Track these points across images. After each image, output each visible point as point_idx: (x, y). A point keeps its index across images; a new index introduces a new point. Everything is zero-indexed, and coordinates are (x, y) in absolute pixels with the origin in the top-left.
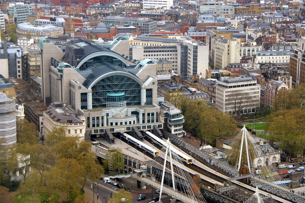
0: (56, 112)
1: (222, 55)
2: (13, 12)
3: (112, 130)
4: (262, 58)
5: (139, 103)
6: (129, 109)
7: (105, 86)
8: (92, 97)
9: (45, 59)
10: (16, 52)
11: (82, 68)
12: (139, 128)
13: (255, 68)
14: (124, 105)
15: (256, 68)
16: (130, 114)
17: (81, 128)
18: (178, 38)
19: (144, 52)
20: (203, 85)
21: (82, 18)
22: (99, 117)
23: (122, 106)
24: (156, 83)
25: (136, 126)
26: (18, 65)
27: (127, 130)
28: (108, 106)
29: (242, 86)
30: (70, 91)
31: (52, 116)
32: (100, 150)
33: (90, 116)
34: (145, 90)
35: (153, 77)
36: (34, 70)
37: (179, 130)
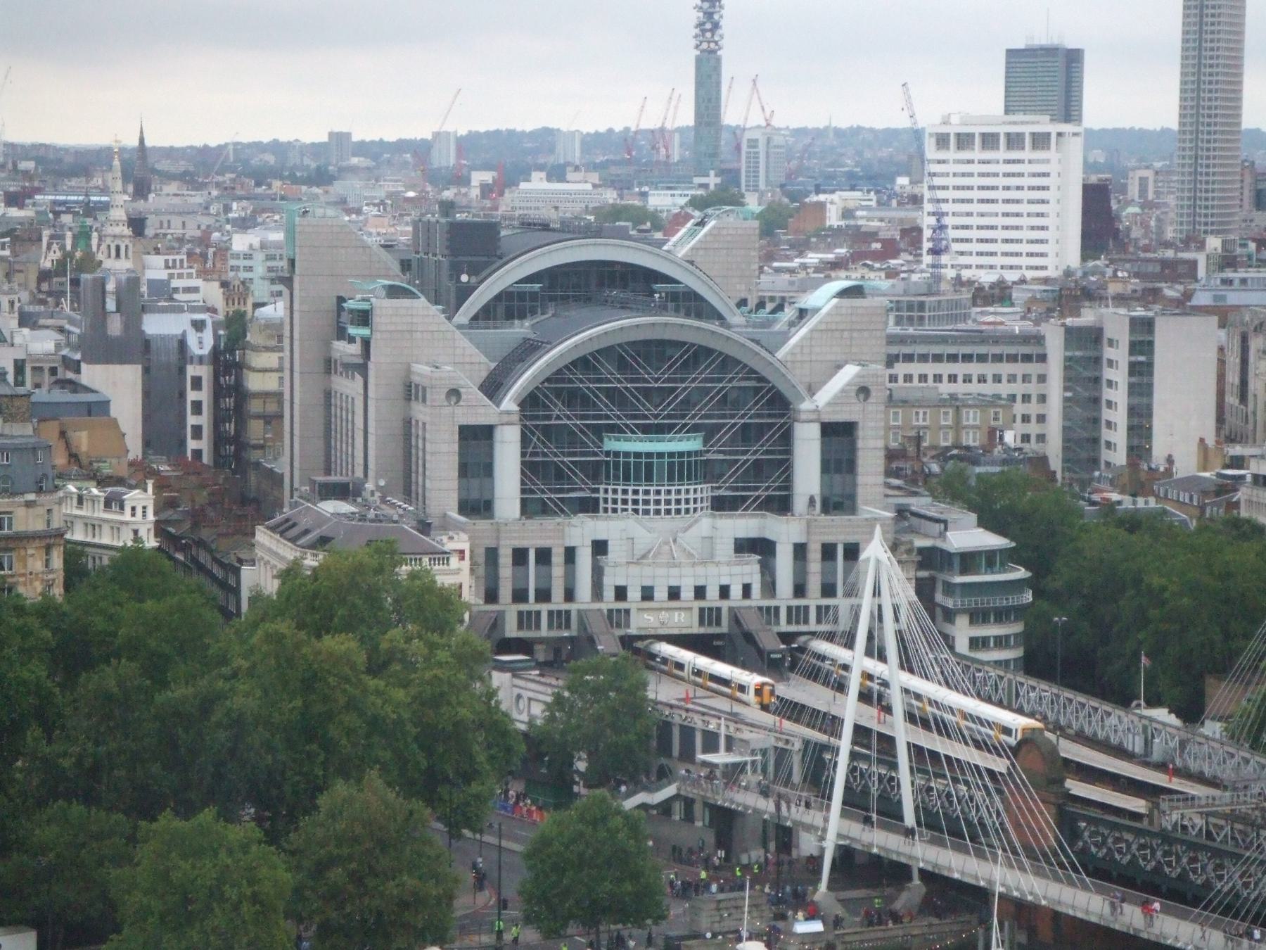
5: (781, 504)
7: (597, 397)
8: (523, 454)
10: (185, 332)
11: (486, 315)
14: (699, 505)
16: (725, 549)
20: (1172, 500)
24: (877, 396)
26: (192, 396)
27: (701, 623)
31: (293, 532)
32: (531, 694)
33: (502, 543)
34: (814, 431)
37: (1001, 642)
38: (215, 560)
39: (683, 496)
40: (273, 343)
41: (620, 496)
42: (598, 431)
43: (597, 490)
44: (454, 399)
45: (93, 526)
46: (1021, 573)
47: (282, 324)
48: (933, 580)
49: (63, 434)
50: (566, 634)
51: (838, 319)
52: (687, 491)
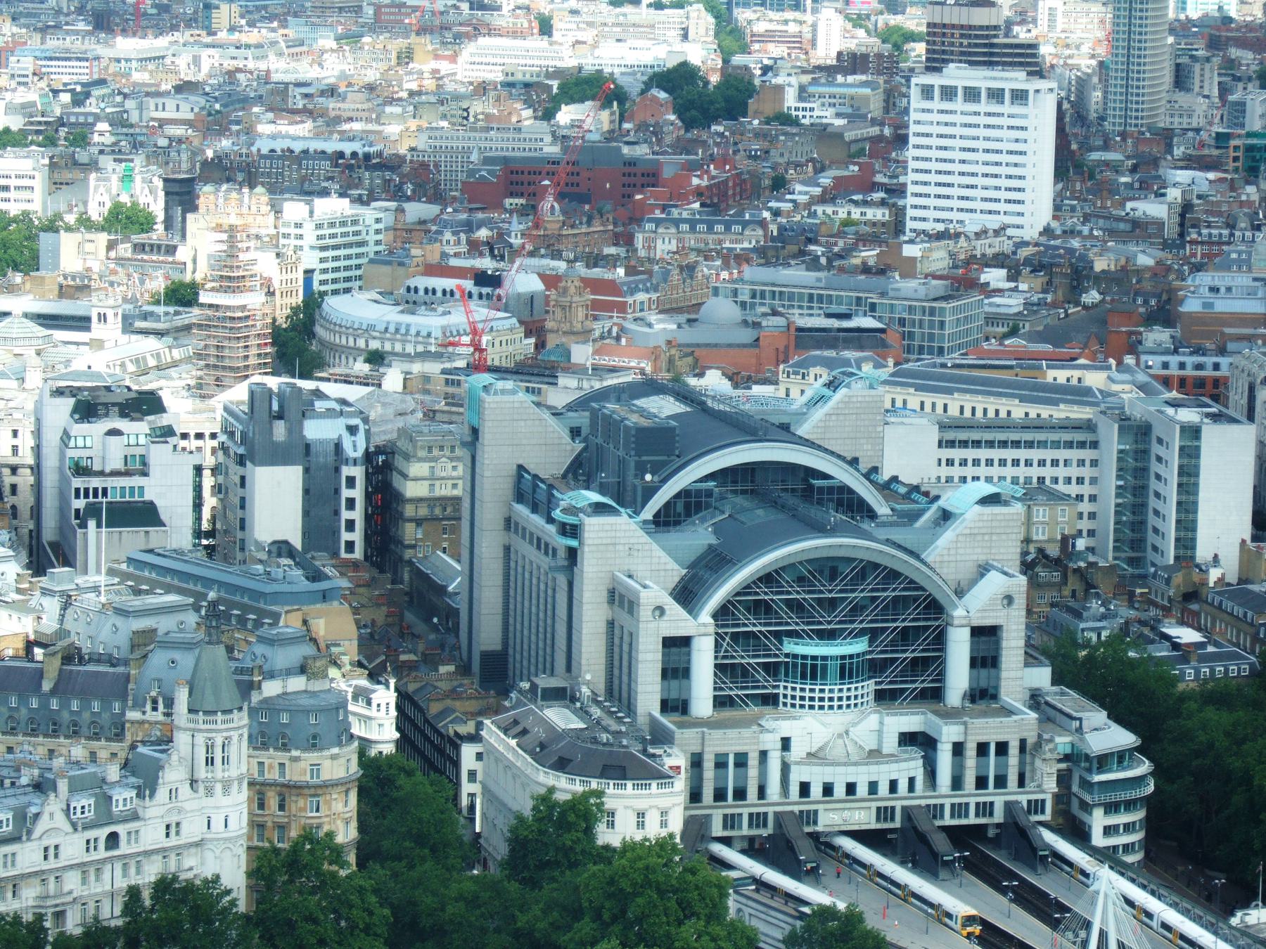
2: (299, 243)
5: (934, 695)
8: (716, 658)
12: (937, 811)
14: (865, 699)
16: (891, 744)
17: (664, 803)
18: (1095, 379)
19: (940, 446)
21: (621, 271)
22: (746, 754)
23: (856, 705)
24: (1020, 602)
26: (346, 493)
27: (878, 819)
28: (789, 701)
32: (753, 912)
33: (707, 749)
34: (966, 632)
35: (1005, 569)
36: (419, 522)
37: (1128, 828)
42: (778, 635)
43: (778, 687)
49: (305, 622)
50: (764, 833)
51: (981, 524)
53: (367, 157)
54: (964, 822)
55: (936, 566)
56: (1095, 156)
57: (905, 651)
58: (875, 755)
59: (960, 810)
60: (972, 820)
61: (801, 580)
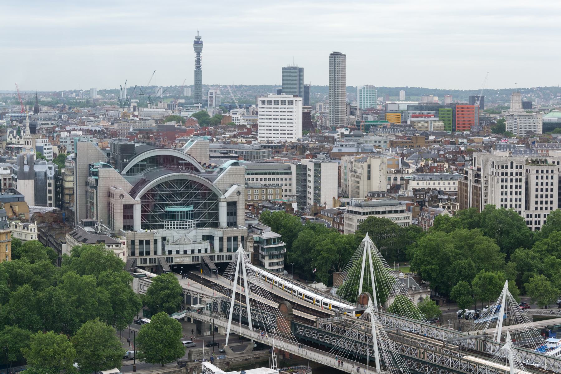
0: (84, 231)
1: (359, 180)
2: (66, 144)
3: (169, 260)
4: (418, 184)
5: (216, 225)
6: (199, 231)
9: (80, 167)
11: (131, 172)
12: (212, 258)
13: (406, 195)
14: (192, 226)
15: (408, 194)
22: (149, 240)
25: (208, 255)
26: (48, 188)
27: (193, 261)
29: (384, 212)
30: (109, 203)
32: (144, 284)
33: (136, 239)
37: (277, 264)
38: (55, 241)
39: (188, 223)
40: (71, 174)
41: (170, 224)
42: (163, 205)
44: (122, 197)
45: (20, 235)
46: (283, 244)
47: (73, 169)
48: (259, 246)
49: (11, 207)
50: (154, 265)
52: (189, 222)
53: (99, 131)
54: (222, 261)
55: (217, 185)
56: (322, 131)
57: (205, 211)
58: (195, 242)
59: (221, 257)
60: (225, 261)
61: (170, 187)
